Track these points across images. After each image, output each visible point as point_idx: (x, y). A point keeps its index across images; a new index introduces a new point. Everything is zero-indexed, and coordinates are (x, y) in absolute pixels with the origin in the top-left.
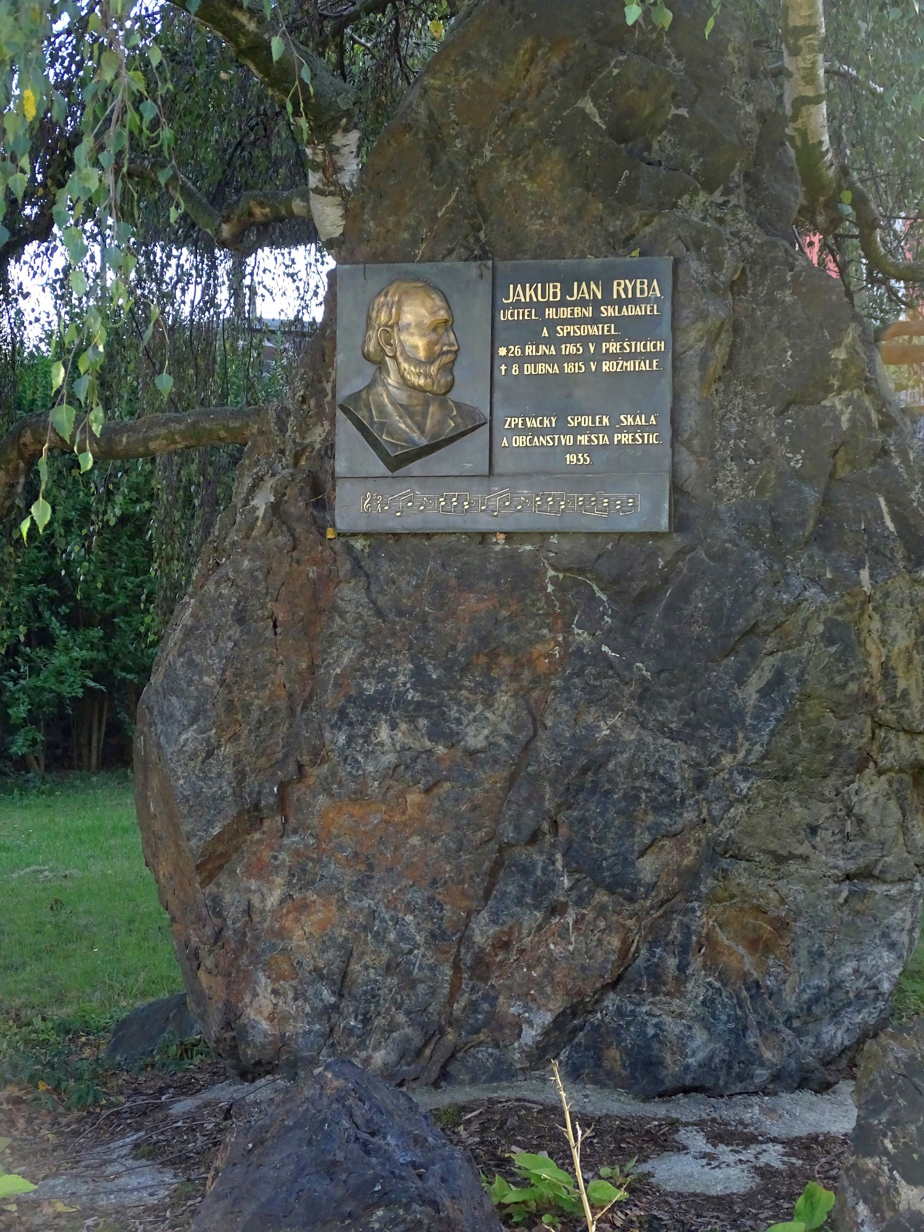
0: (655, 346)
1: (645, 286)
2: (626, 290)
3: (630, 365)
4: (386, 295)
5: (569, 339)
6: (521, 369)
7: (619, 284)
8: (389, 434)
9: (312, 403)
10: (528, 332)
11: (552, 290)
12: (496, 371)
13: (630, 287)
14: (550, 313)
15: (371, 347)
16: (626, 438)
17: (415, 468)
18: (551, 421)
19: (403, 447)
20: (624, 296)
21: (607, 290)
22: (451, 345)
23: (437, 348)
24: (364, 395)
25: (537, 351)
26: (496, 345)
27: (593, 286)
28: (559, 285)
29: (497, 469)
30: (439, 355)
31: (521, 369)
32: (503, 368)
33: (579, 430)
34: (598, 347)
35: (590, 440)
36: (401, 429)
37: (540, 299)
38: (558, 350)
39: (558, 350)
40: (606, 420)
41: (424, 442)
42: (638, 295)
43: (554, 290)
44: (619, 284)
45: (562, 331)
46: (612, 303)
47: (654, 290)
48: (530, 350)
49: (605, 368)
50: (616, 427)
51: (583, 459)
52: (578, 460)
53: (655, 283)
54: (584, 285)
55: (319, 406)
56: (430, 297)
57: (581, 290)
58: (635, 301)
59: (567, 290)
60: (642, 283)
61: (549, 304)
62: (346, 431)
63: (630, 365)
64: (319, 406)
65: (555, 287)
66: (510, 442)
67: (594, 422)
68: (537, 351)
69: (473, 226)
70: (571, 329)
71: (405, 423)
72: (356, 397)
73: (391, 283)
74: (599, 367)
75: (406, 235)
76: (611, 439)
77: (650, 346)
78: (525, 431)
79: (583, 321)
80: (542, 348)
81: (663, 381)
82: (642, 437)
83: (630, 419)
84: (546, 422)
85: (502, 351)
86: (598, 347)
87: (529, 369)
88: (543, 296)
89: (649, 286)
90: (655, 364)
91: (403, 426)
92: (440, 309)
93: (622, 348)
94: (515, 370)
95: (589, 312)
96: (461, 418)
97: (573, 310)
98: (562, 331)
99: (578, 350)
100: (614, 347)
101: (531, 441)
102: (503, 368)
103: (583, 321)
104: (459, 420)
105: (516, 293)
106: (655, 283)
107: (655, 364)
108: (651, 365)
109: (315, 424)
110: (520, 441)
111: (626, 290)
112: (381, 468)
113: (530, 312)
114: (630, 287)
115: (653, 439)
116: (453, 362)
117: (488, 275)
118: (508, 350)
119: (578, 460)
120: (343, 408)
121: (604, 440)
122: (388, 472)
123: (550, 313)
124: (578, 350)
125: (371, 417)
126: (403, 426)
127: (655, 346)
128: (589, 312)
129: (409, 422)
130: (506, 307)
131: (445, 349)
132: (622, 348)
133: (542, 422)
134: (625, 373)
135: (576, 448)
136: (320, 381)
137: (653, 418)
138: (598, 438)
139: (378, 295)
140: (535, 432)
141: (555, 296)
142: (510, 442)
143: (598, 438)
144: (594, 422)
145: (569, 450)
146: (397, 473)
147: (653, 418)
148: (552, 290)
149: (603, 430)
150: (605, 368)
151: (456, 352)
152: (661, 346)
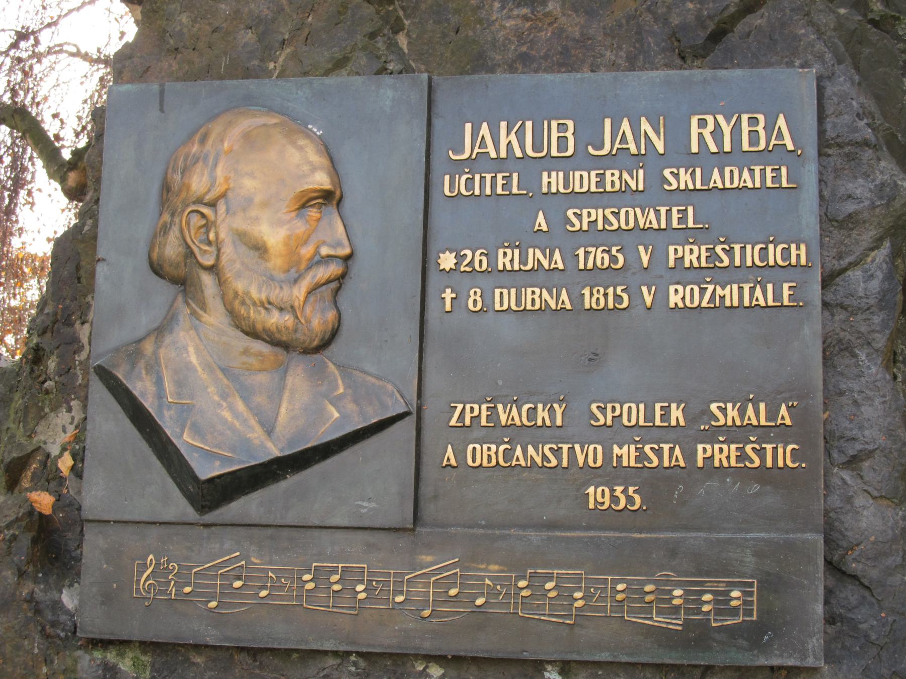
0: (786, 253)
1: (760, 128)
2: (717, 133)
3: (730, 294)
4: (203, 140)
5: (595, 235)
6: (487, 297)
7: (702, 123)
8: (197, 430)
9: (52, 364)
10: (504, 221)
11: (555, 135)
12: (432, 304)
13: (727, 129)
14: (553, 181)
15: (171, 249)
16: (724, 454)
17: (249, 506)
18: (552, 411)
19: (229, 460)
20: (713, 148)
21: (677, 135)
22: (339, 244)
23: (307, 251)
24: (148, 347)
25: (523, 261)
26: (433, 248)
27: (645, 126)
28: (570, 124)
29: (429, 510)
30: (309, 268)
31: (487, 297)
32: (448, 295)
33: (616, 432)
34: (658, 256)
35: (641, 456)
36: (224, 421)
37: (530, 152)
38: (570, 257)
39: (570, 257)
40: (677, 414)
41: (274, 451)
42: (746, 147)
43: (561, 135)
44: (702, 123)
45: (581, 219)
46: (691, 161)
47: (780, 135)
48: (506, 259)
49: (674, 299)
50: (700, 428)
51: (629, 497)
52: (615, 499)
53: (781, 122)
54: (625, 126)
55: (66, 370)
56: (294, 143)
57: (617, 135)
58: (736, 157)
59: (589, 135)
60: (753, 121)
61: (550, 163)
62: (109, 423)
63: (730, 294)
64: (66, 370)
65: (562, 127)
66: (460, 454)
67: (650, 416)
68: (523, 261)
69: (386, 20)
70: (597, 214)
71: (232, 408)
72: (133, 352)
73: (213, 118)
74: (661, 296)
75: (249, 37)
76: (690, 456)
77: (775, 254)
78: (495, 431)
79: (625, 195)
80: (535, 255)
81: (807, 331)
82: (761, 453)
83: (732, 412)
84: (542, 414)
85: (447, 261)
86: (658, 256)
87: (505, 298)
88: (537, 147)
89: (769, 129)
90: (786, 293)
91: (227, 415)
92: (314, 169)
93: (712, 255)
94: (474, 300)
95: (637, 181)
96: (356, 401)
97: (602, 176)
98: (581, 219)
99: (613, 259)
100: (694, 254)
101: (508, 455)
102: (448, 295)
103: (625, 195)
104: (351, 407)
105: (478, 138)
106: (781, 122)
107: (786, 293)
108: (778, 296)
109: (55, 409)
110: (483, 454)
111: (717, 133)
112: (179, 506)
113: (508, 179)
114: (727, 129)
115: (784, 455)
116: (341, 278)
117: (418, 98)
118: (460, 258)
119: (615, 499)
120: (106, 377)
121: (672, 455)
122: (191, 513)
123: (553, 181)
124: (613, 259)
125: (160, 395)
126: (227, 415)
127: (786, 253)
128: (637, 181)
129: (240, 406)
130: (458, 167)
131: (325, 251)
132: (712, 255)
133: (532, 413)
134: (719, 308)
135: (610, 473)
136: (69, 323)
137: (783, 410)
138: (659, 453)
139: (190, 137)
140: (517, 434)
141: (562, 141)
142: (460, 454)
143: (659, 453)
144: (650, 416)
145: (594, 475)
146: (209, 518)
147: (783, 410)
148: (555, 135)
149: (669, 432)
150: (674, 299)
151: (347, 258)
152: (799, 254)
